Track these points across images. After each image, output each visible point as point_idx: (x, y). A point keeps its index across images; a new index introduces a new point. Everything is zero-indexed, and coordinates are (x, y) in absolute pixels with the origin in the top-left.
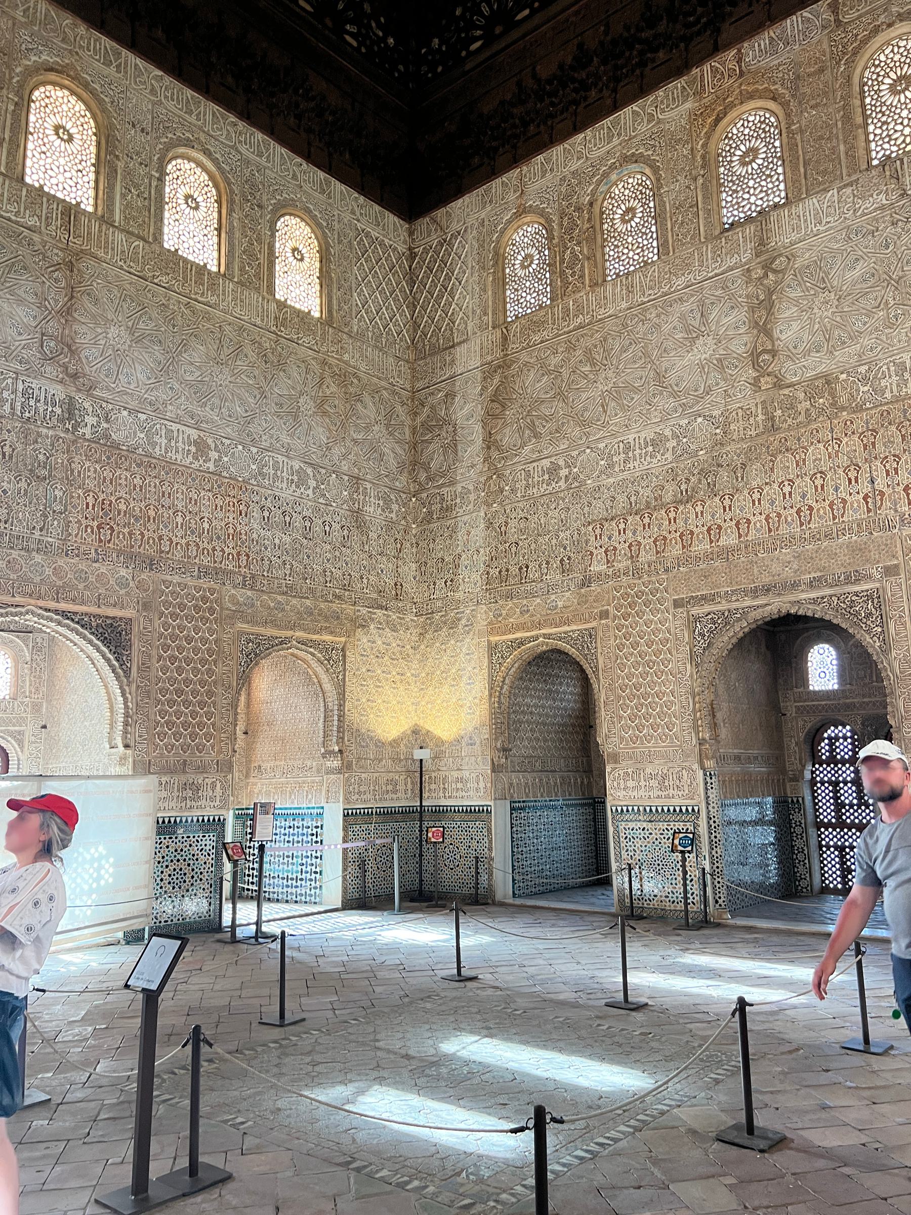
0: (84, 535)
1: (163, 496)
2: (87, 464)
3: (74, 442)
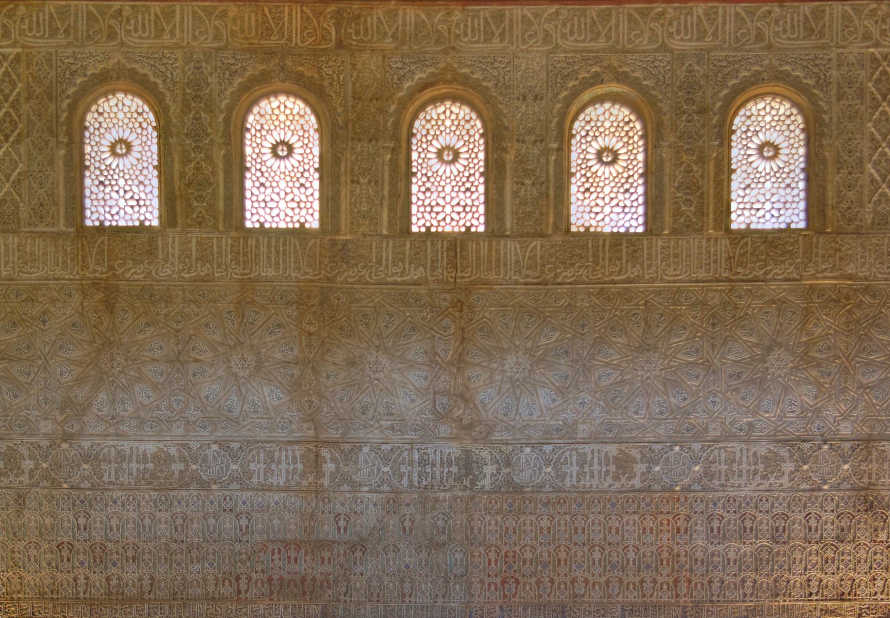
0: (488, 594)
1: (576, 532)
2: (488, 517)
3: (472, 498)
